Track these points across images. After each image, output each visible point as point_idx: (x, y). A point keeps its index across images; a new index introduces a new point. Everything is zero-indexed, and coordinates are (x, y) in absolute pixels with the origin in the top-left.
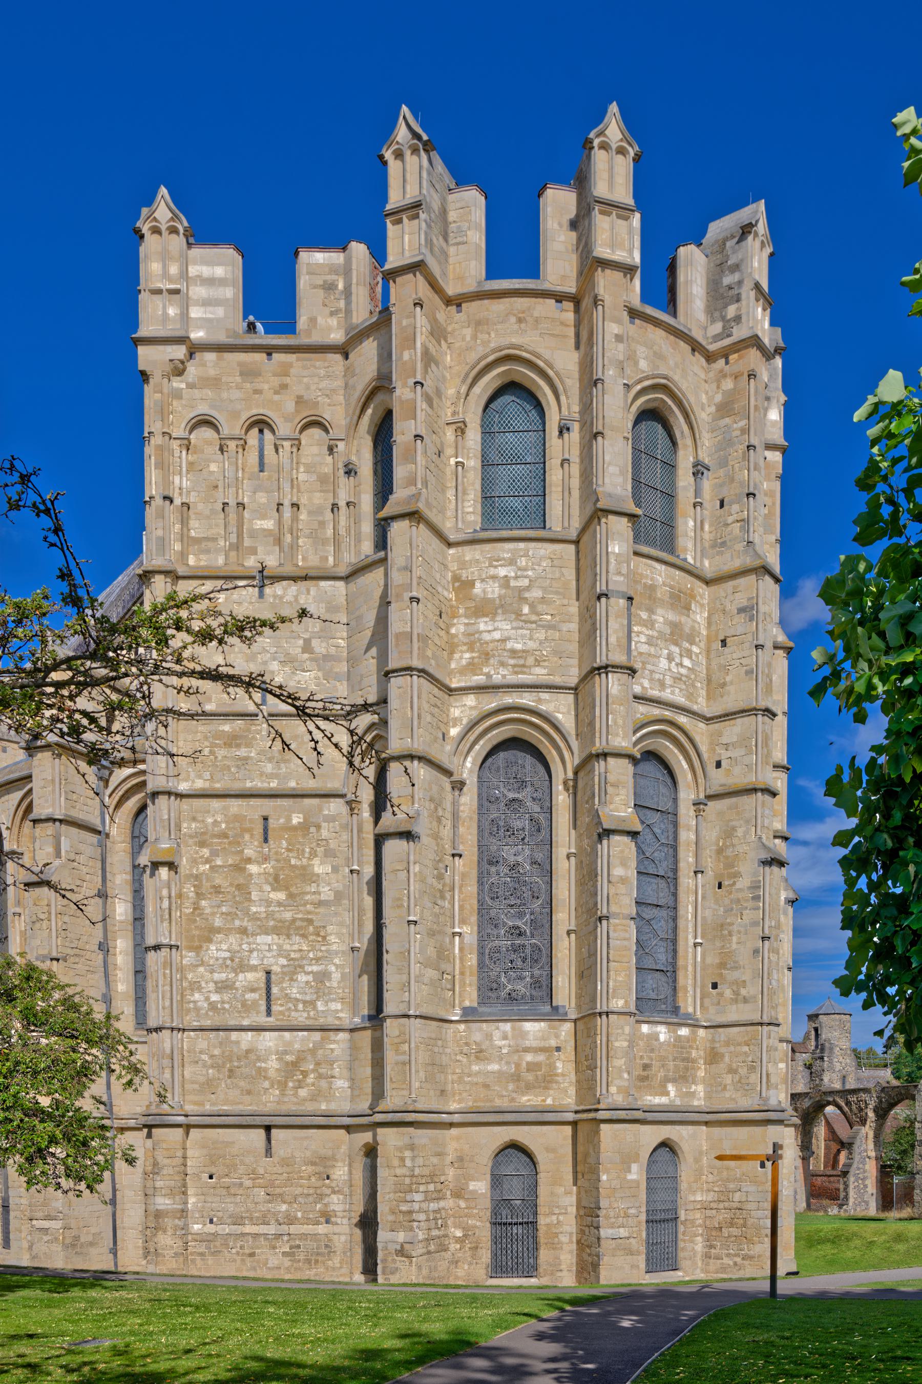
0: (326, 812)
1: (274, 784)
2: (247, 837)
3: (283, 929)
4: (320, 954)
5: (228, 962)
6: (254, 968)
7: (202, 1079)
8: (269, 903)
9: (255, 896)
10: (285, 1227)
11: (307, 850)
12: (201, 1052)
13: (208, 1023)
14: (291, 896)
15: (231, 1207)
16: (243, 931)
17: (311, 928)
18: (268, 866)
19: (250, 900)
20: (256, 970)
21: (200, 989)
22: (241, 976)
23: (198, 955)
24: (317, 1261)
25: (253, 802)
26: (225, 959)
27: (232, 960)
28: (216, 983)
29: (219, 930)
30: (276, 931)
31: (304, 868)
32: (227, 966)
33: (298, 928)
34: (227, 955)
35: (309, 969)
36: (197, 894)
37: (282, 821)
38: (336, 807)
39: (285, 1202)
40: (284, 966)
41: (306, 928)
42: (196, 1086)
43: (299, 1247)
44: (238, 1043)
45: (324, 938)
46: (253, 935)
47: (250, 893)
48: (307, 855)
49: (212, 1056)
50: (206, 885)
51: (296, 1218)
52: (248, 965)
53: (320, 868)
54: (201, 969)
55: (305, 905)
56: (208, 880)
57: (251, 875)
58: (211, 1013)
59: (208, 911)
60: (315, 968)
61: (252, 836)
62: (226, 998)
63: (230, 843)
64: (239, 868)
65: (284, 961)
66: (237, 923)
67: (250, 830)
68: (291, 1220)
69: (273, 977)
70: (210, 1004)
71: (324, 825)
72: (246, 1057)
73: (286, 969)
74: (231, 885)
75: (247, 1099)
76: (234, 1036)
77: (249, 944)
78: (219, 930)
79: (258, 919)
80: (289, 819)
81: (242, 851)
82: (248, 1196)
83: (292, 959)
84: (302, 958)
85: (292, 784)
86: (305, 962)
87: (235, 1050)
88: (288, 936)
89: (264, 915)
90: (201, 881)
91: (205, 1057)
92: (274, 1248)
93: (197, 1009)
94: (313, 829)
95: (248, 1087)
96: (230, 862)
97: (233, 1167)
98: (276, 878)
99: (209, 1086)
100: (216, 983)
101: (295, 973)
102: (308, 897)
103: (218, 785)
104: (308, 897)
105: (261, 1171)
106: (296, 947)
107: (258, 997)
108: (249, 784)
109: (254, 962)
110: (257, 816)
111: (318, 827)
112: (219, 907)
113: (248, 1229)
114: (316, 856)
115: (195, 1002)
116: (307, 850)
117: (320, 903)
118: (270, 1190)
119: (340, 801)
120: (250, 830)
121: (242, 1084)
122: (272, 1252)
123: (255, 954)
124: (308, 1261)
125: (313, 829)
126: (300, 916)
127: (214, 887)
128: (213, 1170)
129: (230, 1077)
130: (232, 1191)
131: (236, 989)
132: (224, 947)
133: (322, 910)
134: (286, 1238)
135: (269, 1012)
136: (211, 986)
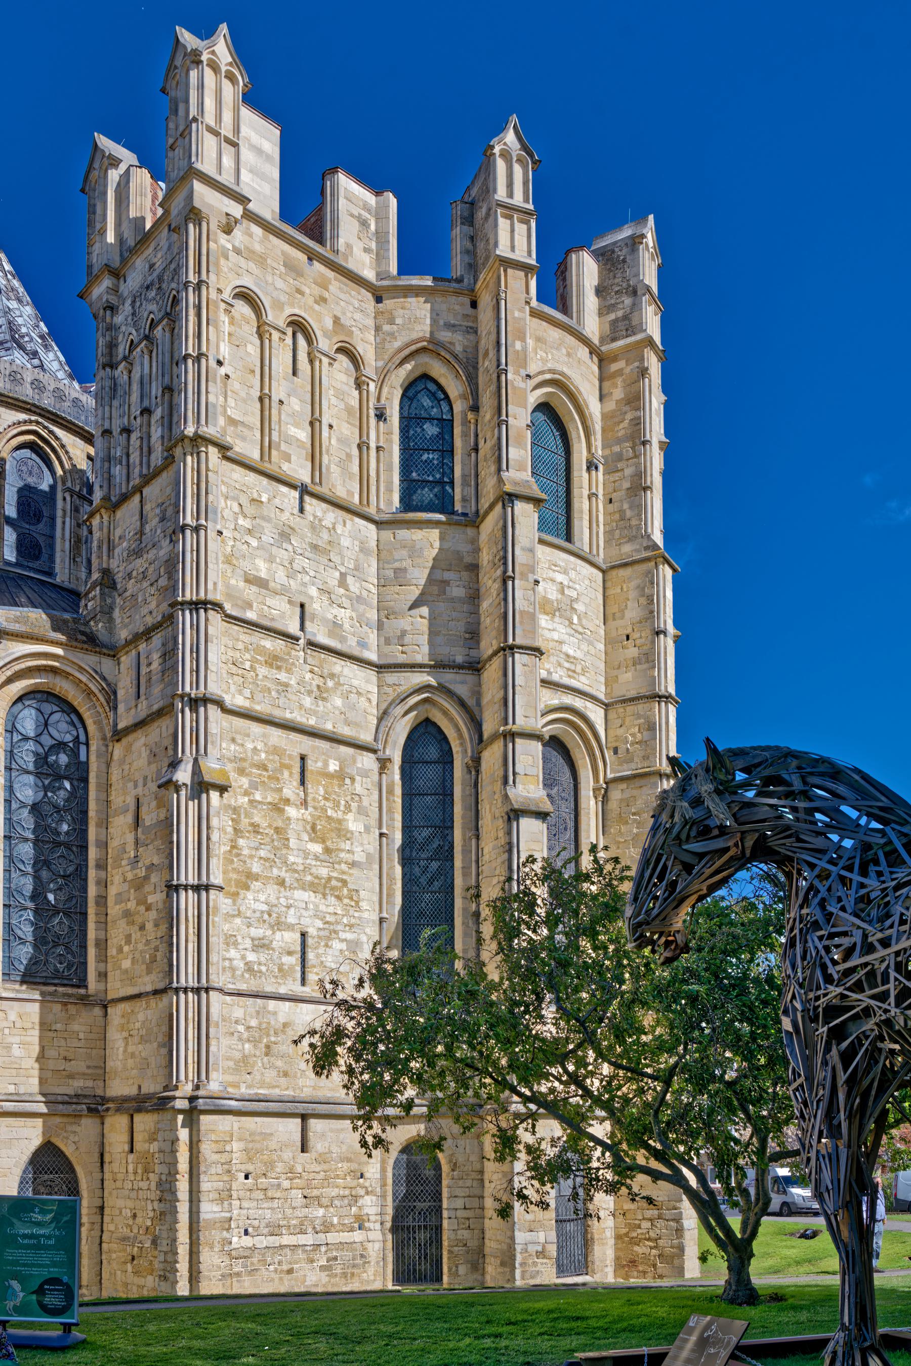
0: (360, 765)
1: (312, 722)
2: (286, 773)
3: (321, 887)
4: (353, 921)
5: (266, 917)
6: (290, 927)
7: (238, 1055)
8: (306, 854)
9: (293, 843)
10: (321, 1236)
11: (343, 803)
12: (236, 1022)
13: (243, 987)
14: (327, 851)
15: (268, 1214)
16: (281, 883)
17: (345, 891)
18: (307, 814)
19: (287, 847)
20: (293, 930)
21: (236, 944)
22: (278, 935)
23: (234, 904)
24: (353, 1274)
25: (294, 736)
26: (262, 912)
27: (270, 915)
28: (253, 939)
29: (256, 877)
30: (313, 887)
31: (340, 821)
32: (264, 921)
33: (333, 889)
34: (265, 908)
35: (343, 935)
36: (235, 829)
37: (320, 764)
38: (368, 761)
39: (321, 1206)
40: (320, 929)
41: (340, 889)
42: (231, 1064)
43: (336, 1258)
44: (275, 1013)
45: (357, 902)
46: (290, 888)
47: (288, 839)
48: (342, 808)
49: (248, 1028)
50: (245, 821)
51: (332, 1225)
52: (285, 923)
53: (354, 824)
54: (238, 921)
55: (339, 863)
56: (246, 816)
57: (289, 819)
58: (247, 976)
59: (246, 852)
60: (349, 936)
61: (291, 774)
62: (262, 959)
63: (269, 777)
64: (277, 808)
65: (319, 924)
66: (275, 872)
67: (289, 767)
68: (327, 1227)
69: (310, 941)
70: (246, 964)
71: (358, 778)
72: (284, 1032)
73: (322, 933)
74: (270, 826)
75: (283, 1081)
76: (272, 1004)
77: (287, 898)
78: (256, 877)
79: (296, 871)
80: (326, 764)
81: (280, 790)
82: (286, 1199)
83: (327, 923)
84: (337, 923)
85: (329, 726)
86: (339, 927)
87: (273, 1023)
88: (324, 896)
89: (301, 868)
90: (239, 816)
91: (241, 1028)
92: (312, 1261)
93: (233, 969)
94: (348, 781)
95: (285, 1068)
96: (269, 799)
97: (271, 1165)
98: (313, 828)
99: (244, 1064)
100: (253, 939)
101: (329, 938)
102: (342, 855)
103: (258, 708)
104: (342, 855)
105: (300, 1169)
106: (331, 910)
107: (293, 960)
108: (288, 715)
109: (291, 920)
110: (296, 753)
111: (353, 780)
112: (257, 849)
113: (287, 1240)
114: (350, 811)
115: (230, 960)
116: (343, 803)
117: (353, 864)
118: (307, 1192)
119: (371, 755)
120: (289, 767)
121: (279, 1063)
122: (309, 1266)
123: (292, 911)
124: (344, 1275)
125: (348, 781)
126: (335, 874)
127: (252, 825)
128: (250, 1168)
129: (267, 1054)
130: (270, 1194)
131: (273, 949)
132: (262, 898)
133: (354, 871)
134: (323, 1249)
135: (303, 982)
136: (248, 943)
